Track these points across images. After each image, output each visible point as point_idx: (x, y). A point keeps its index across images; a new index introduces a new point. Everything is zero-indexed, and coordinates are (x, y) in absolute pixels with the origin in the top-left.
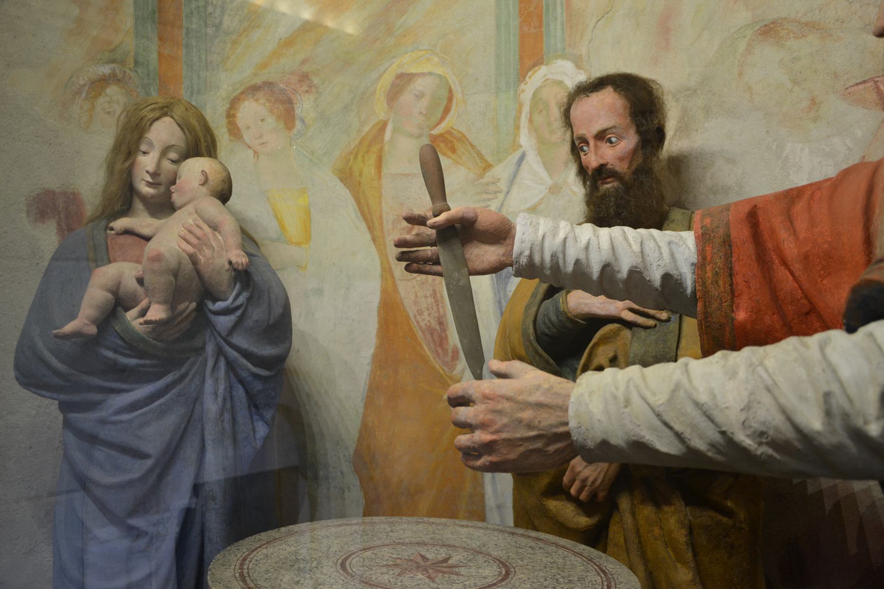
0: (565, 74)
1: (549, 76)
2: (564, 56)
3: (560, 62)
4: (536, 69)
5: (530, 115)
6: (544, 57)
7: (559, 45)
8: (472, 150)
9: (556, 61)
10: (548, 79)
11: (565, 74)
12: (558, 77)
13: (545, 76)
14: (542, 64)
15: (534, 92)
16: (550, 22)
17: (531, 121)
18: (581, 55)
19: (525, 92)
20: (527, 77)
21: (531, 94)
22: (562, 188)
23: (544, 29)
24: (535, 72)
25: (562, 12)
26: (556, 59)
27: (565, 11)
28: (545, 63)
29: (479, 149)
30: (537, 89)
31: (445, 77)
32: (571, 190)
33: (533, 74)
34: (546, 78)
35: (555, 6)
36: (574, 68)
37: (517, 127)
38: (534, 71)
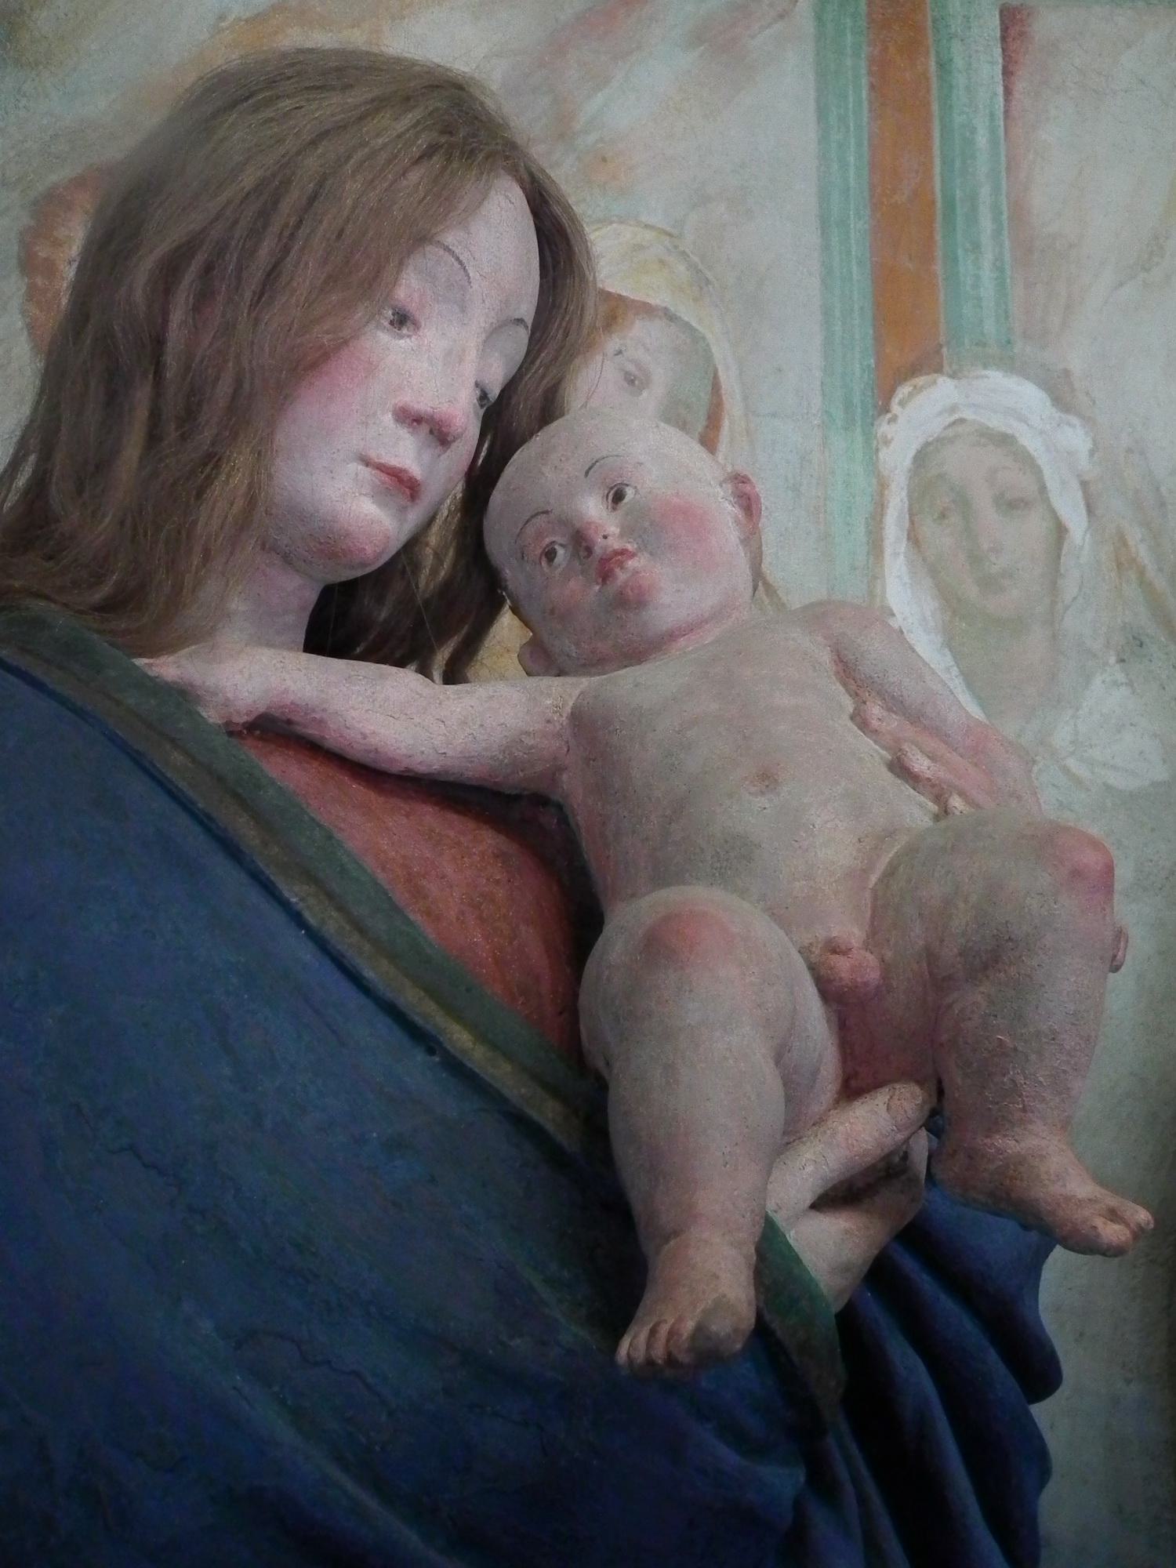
0: (1024, 420)
1: (968, 415)
2: (1010, 364)
3: (995, 377)
4: (921, 380)
5: (912, 522)
6: (944, 350)
7: (990, 326)
8: (766, 601)
9: (987, 372)
10: (962, 421)
11: (1024, 420)
12: (996, 423)
13: (953, 409)
14: (939, 370)
15: (919, 452)
16: (960, 252)
17: (914, 538)
18: (1067, 373)
19: (892, 445)
20: (895, 401)
21: (912, 453)
22: (1034, 762)
23: (939, 268)
24: (918, 390)
25: (997, 233)
26: (985, 367)
27: (1005, 232)
28: (946, 368)
29: (784, 599)
30: (927, 444)
31: (704, 338)
32: (1066, 770)
33: (911, 395)
34: (956, 416)
35: (974, 208)
36: (1048, 403)
37: (876, 546)
38: (915, 387)
